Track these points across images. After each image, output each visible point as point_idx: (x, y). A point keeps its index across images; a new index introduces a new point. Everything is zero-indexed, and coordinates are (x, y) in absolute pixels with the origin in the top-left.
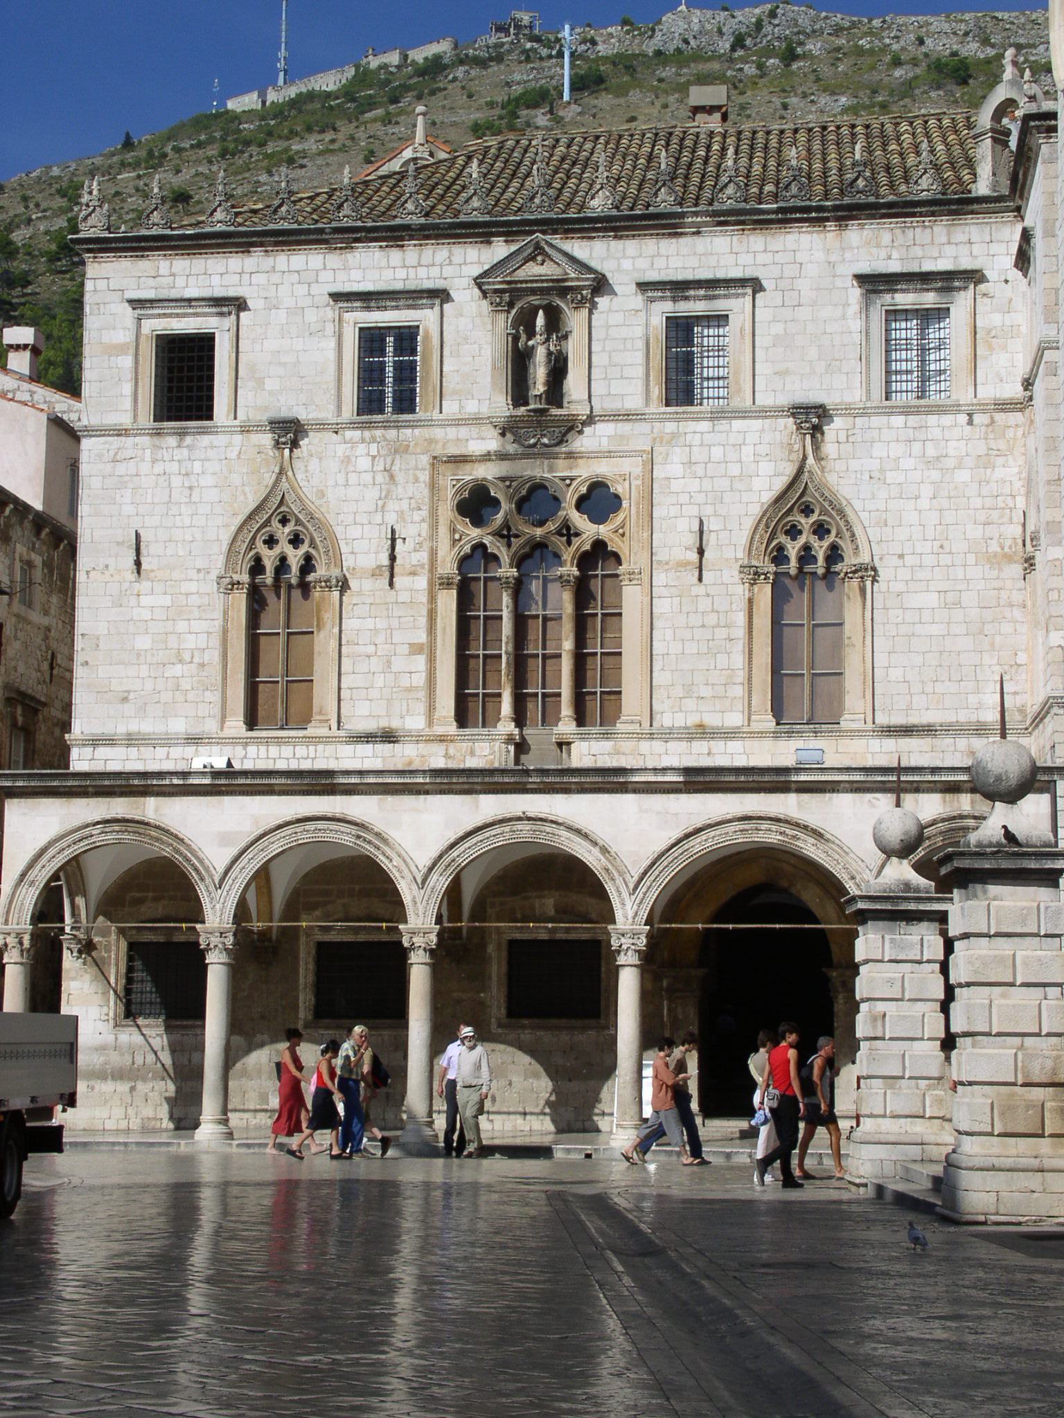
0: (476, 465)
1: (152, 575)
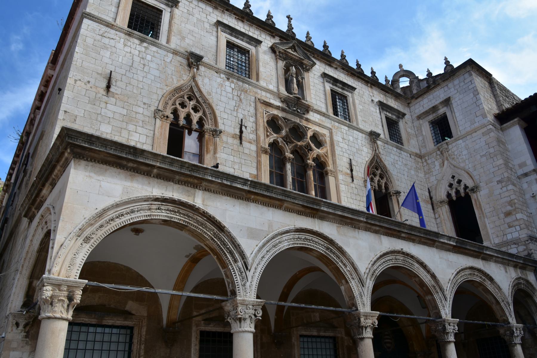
0: (274, 109)
1: (116, 96)
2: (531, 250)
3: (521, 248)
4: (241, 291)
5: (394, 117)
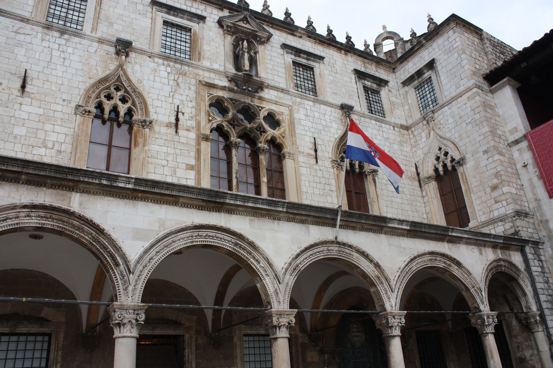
0: (218, 91)
1: (32, 96)
2: (518, 227)
3: (508, 225)
4: (122, 295)
5: (375, 86)
